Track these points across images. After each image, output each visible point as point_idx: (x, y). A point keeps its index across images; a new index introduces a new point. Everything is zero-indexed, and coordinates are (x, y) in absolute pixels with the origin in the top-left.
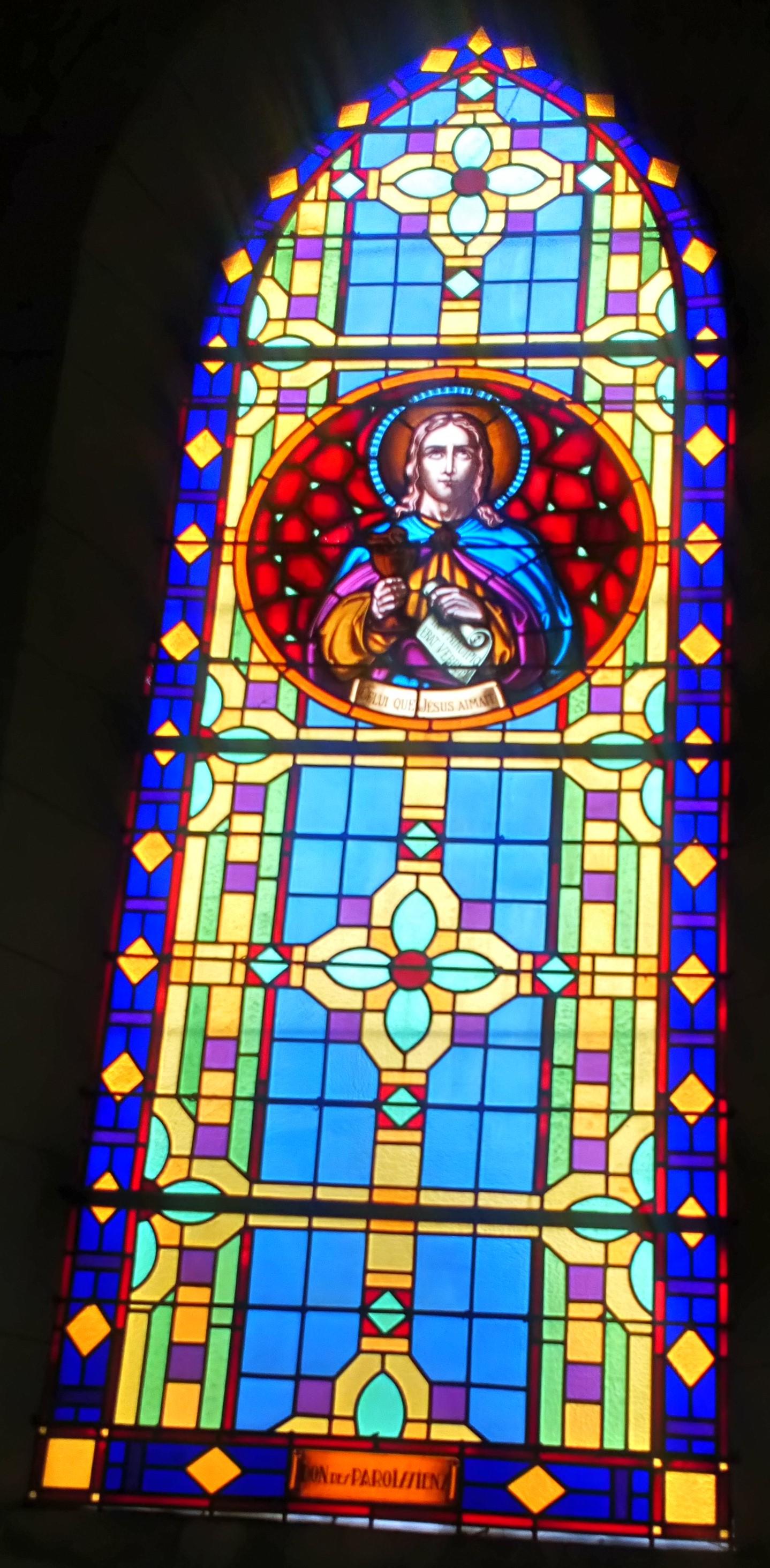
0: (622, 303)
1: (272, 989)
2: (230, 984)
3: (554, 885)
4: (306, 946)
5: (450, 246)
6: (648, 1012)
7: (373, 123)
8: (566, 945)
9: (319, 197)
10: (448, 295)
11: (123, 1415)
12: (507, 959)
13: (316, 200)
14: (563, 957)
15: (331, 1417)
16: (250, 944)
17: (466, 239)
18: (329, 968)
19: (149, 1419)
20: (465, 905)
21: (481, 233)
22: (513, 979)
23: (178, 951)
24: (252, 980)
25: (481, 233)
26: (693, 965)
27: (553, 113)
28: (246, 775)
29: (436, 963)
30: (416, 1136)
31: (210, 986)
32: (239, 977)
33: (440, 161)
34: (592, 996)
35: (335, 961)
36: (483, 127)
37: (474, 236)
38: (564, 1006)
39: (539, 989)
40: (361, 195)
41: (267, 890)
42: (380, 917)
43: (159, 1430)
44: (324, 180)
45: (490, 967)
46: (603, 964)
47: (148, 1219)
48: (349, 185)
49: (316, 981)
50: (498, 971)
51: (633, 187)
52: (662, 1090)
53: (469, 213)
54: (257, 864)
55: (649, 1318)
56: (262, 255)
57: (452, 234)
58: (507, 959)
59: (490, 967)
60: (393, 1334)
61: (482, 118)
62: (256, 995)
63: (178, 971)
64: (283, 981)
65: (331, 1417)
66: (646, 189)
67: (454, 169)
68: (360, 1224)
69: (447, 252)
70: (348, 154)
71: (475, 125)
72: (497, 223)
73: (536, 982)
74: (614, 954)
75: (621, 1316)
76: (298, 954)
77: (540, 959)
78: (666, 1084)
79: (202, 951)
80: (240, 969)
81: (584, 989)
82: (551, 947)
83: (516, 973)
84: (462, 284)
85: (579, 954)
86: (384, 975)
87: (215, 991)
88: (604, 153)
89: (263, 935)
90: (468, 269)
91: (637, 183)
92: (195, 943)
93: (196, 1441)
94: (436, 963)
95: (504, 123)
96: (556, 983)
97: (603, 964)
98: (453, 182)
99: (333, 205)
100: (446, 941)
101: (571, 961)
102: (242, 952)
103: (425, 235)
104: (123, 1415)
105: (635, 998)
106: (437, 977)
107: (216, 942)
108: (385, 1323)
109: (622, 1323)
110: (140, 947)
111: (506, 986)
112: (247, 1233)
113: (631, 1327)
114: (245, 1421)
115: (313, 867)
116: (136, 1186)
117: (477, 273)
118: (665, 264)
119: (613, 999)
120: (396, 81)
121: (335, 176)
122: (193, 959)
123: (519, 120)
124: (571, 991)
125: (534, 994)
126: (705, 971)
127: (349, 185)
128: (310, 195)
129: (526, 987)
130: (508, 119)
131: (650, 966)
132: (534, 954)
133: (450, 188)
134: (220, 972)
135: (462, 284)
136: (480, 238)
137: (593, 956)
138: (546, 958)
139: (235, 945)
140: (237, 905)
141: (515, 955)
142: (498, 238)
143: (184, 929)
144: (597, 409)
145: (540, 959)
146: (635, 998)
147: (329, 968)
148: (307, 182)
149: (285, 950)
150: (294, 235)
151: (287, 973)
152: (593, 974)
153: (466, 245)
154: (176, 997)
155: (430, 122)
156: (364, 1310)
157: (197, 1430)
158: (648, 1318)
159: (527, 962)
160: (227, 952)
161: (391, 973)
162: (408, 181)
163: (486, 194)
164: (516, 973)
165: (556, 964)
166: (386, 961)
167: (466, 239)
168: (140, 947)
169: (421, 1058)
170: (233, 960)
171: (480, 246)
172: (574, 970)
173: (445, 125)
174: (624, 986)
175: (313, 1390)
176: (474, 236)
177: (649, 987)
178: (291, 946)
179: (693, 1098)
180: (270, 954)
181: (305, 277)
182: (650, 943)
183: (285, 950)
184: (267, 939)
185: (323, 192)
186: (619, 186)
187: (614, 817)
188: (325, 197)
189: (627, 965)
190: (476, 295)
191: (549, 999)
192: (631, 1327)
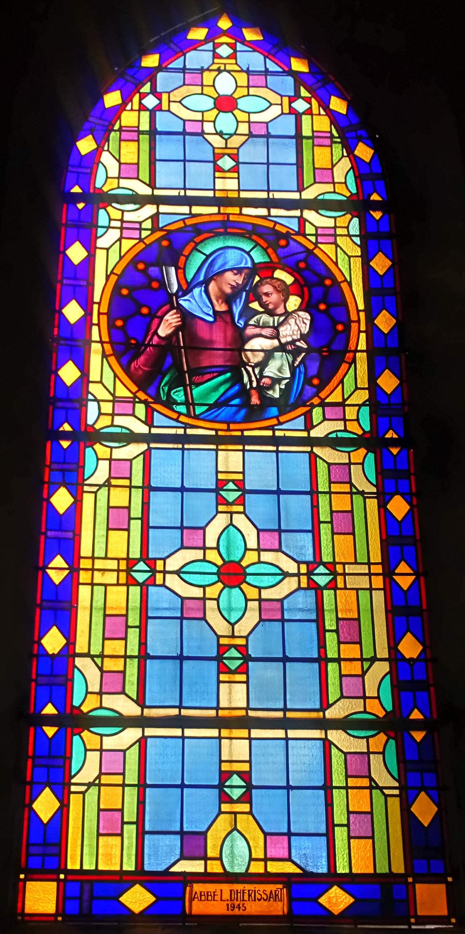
0: (325, 175)
1: (144, 587)
2: (118, 584)
3: (316, 522)
4: (164, 559)
5: (217, 141)
6: (379, 597)
7: (164, 65)
8: (327, 558)
9: (134, 108)
10: (217, 169)
11: (72, 864)
12: (291, 567)
13: (132, 110)
14: (325, 565)
15: (205, 858)
16: (128, 559)
17: (226, 137)
18: (182, 575)
19: (88, 866)
20: (261, 533)
21: (235, 134)
22: (296, 579)
23: (84, 564)
24: (131, 582)
25: (235, 134)
26: (403, 567)
27: (272, 67)
28: (118, 454)
29: (248, 571)
30: (243, 677)
31: (106, 585)
32: (123, 580)
33: (206, 90)
34: (345, 588)
35: (184, 570)
36: (229, 72)
37: (231, 135)
38: (328, 595)
39: (313, 586)
40: (159, 108)
41: (136, 526)
42: (211, 542)
43: (97, 871)
44: (136, 98)
45: (279, 572)
46: (349, 569)
47: (79, 734)
48: (151, 102)
49: (172, 581)
50: (286, 575)
51: (322, 112)
52: (392, 645)
53: (226, 122)
54: (129, 508)
55: (396, 784)
56: (102, 140)
57: (217, 133)
58: (291, 567)
59: (279, 572)
60: (240, 800)
61: (228, 67)
62: (135, 591)
63: (84, 577)
64: (151, 581)
65: (205, 858)
66: (329, 113)
67: (216, 96)
68: (214, 732)
69: (215, 145)
70: (149, 84)
71: (225, 70)
72: (244, 129)
73: (310, 580)
74: (356, 563)
75: (380, 785)
76: (159, 565)
77: (312, 566)
78: (394, 640)
79: (99, 564)
80: (123, 575)
81: (340, 584)
82: (318, 560)
83: (298, 575)
84: (227, 163)
85: (334, 563)
86: (215, 578)
87: (109, 588)
88: (304, 93)
89: (135, 553)
90: (229, 155)
91: (324, 110)
92: (93, 558)
93: (122, 880)
94: (248, 571)
95: (242, 71)
96: (322, 581)
97: (349, 569)
98: (215, 103)
99: (142, 113)
100: (252, 557)
101: (331, 567)
102: (123, 565)
103: (202, 134)
104: (72, 864)
105: (371, 589)
106: (249, 579)
107: (106, 558)
108: (236, 794)
109: (381, 789)
110: (59, 561)
111: (291, 584)
112: (142, 742)
113: (387, 792)
114: (151, 865)
115: (164, 508)
116: (68, 710)
117: (235, 157)
118: (345, 154)
119: (357, 590)
120: (174, 46)
121: (143, 96)
122: (93, 570)
123: (251, 69)
124: (332, 586)
125: (308, 588)
126: (410, 571)
127: (151, 102)
128: (129, 107)
129: (304, 584)
130: (245, 69)
131: (378, 569)
132: (307, 563)
133: (213, 106)
134: (111, 578)
135: (227, 163)
136: (234, 137)
137: (344, 564)
138: (316, 565)
139: (118, 559)
140: (118, 540)
141: (296, 565)
142: (247, 137)
143: (85, 550)
144: (313, 239)
145: (312, 566)
146: (371, 589)
147: (181, 575)
148: (127, 99)
149: (151, 563)
150: (121, 130)
151: (153, 577)
152: (344, 574)
153: (226, 140)
154: (84, 592)
155: (199, 67)
156: (221, 787)
157: (121, 872)
158: (396, 784)
159: (304, 569)
160: (113, 565)
161: (218, 577)
162: (189, 104)
163: (236, 112)
164: (298, 575)
165: (321, 569)
166: (215, 570)
167: (226, 137)
168: (59, 561)
169: (243, 629)
170: (118, 571)
171: (235, 142)
172: (333, 573)
173: (208, 69)
174: (364, 582)
175: (193, 843)
176: (231, 135)
177: (378, 582)
178: (155, 560)
179: (410, 647)
180: (141, 566)
181: (129, 152)
182: (376, 556)
183: (151, 563)
184: (138, 556)
185: (136, 106)
186: (315, 111)
187: (347, 480)
188: (137, 108)
189: (364, 569)
190: (235, 169)
191: (318, 590)
192: (387, 792)
